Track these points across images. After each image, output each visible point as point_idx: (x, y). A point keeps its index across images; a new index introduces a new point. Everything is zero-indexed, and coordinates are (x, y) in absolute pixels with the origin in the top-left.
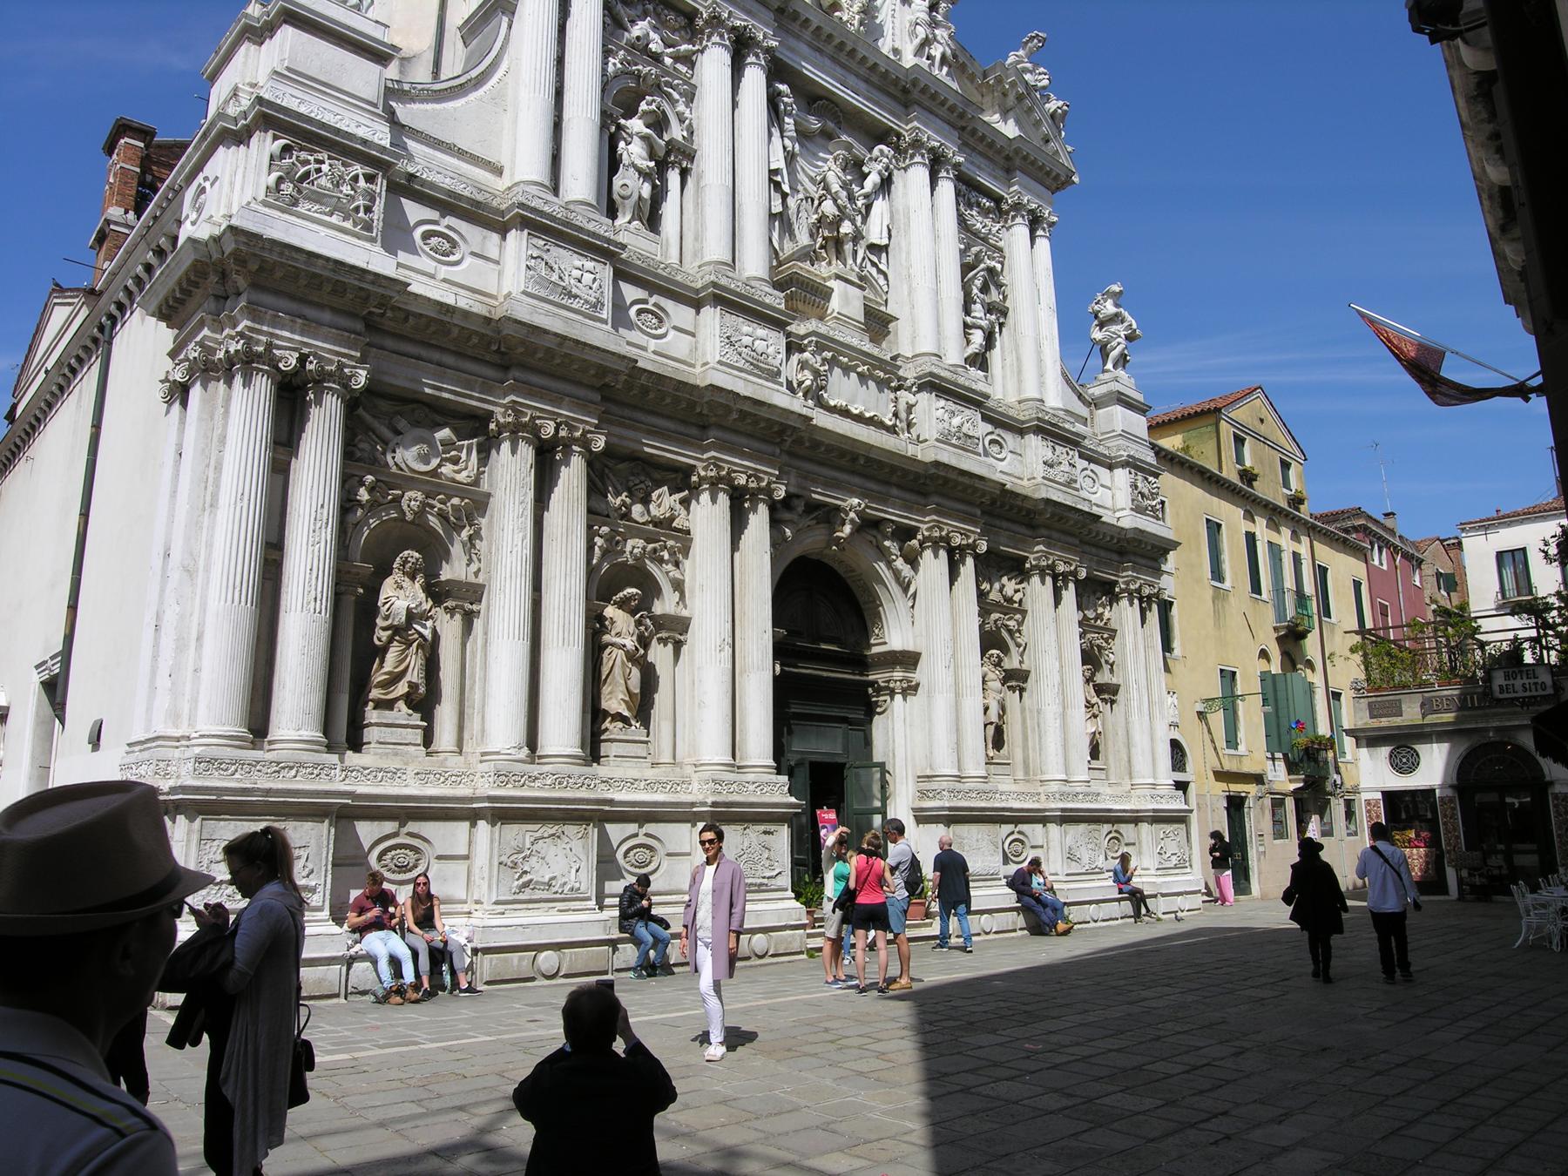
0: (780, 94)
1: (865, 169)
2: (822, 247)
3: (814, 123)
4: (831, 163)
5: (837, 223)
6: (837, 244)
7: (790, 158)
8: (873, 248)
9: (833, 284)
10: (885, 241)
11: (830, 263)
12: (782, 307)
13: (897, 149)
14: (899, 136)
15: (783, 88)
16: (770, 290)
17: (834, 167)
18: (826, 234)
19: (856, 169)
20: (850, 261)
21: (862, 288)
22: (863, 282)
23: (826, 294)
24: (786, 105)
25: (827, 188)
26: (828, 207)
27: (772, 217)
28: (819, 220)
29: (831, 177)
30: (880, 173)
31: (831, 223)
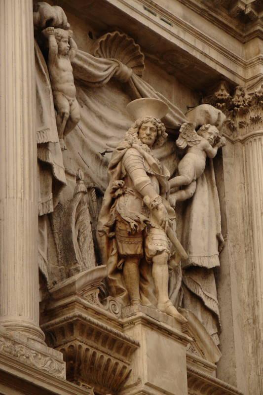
0: (50, 22)
1: (181, 143)
2: (118, 271)
3: (102, 67)
4: (131, 135)
5: (142, 233)
6: (145, 263)
7: (66, 124)
8: (192, 270)
9: (138, 334)
10: (214, 262)
11: (129, 300)
12: (63, 375)
13: (230, 108)
14: (232, 88)
15: (56, 12)
16: (40, 346)
17: (137, 144)
18: (128, 249)
19: (169, 140)
20: (164, 297)
21: (182, 340)
22: (184, 335)
23: (129, 348)
24: (59, 39)
25: (125, 177)
26: (128, 207)
27: (41, 218)
28: (113, 228)
29: (133, 158)
30: (205, 150)
31: (132, 234)
